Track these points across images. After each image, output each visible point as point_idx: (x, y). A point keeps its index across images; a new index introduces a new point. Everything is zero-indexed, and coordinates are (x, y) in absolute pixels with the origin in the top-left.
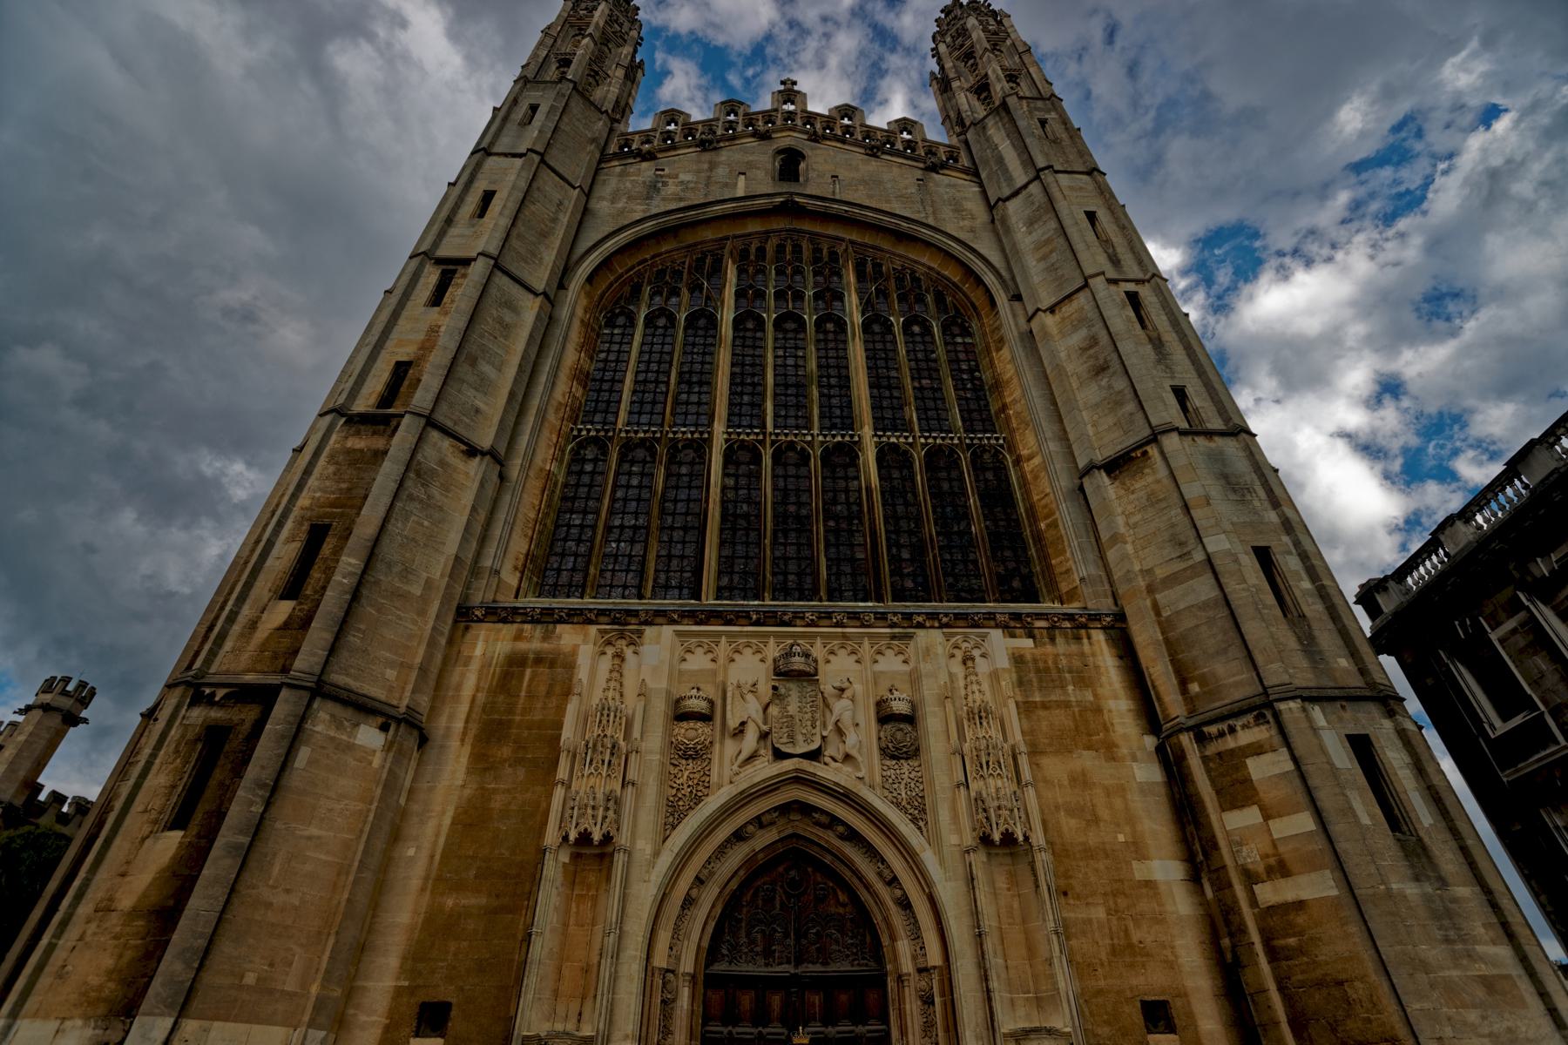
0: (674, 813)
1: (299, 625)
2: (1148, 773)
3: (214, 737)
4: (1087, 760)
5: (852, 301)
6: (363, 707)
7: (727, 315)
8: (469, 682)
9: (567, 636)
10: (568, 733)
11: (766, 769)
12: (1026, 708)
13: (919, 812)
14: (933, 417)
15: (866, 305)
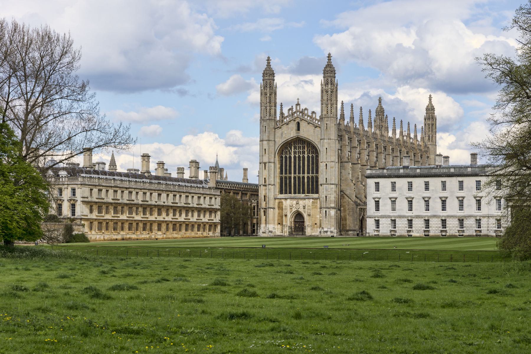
0: (291, 212)
1: (266, 204)
2: (319, 210)
3: (264, 211)
4: (315, 209)
5: (306, 153)
6: (271, 208)
7: (292, 156)
8: (277, 204)
9: (282, 200)
10: (284, 208)
11: (296, 210)
12: (312, 205)
13: (305, 213)
14: (313, 173)
15: (308, 154)
